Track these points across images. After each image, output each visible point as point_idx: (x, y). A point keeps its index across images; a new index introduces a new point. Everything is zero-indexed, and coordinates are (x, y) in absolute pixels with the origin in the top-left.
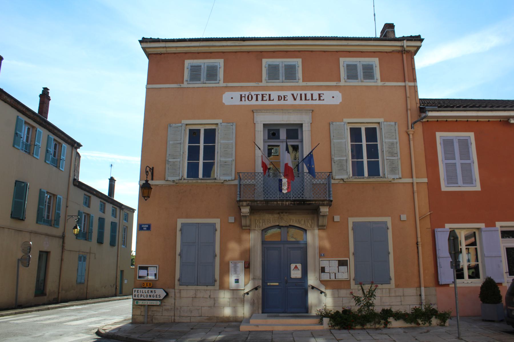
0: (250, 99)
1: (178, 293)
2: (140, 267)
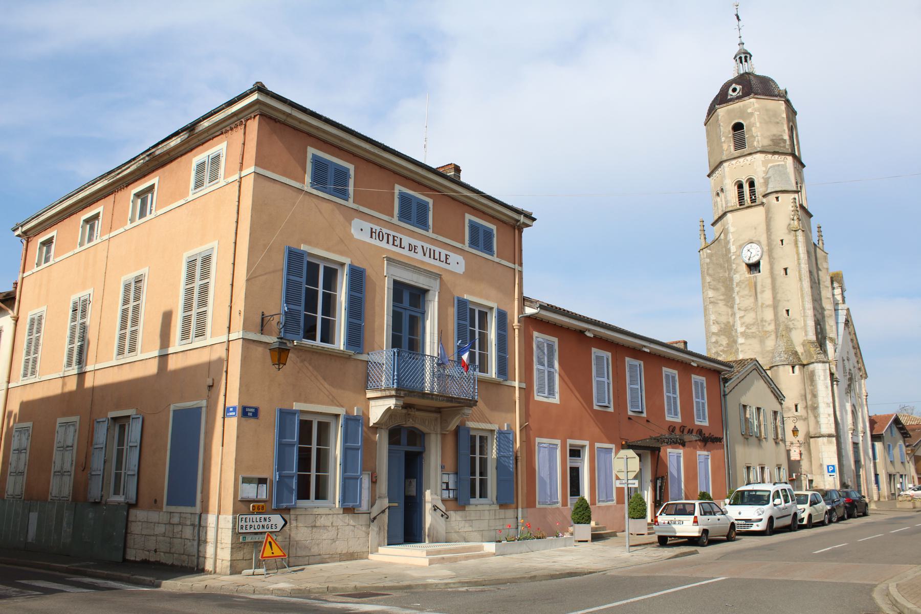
0: (381, 239)
1: (293, 520)
2: (243, 478)
